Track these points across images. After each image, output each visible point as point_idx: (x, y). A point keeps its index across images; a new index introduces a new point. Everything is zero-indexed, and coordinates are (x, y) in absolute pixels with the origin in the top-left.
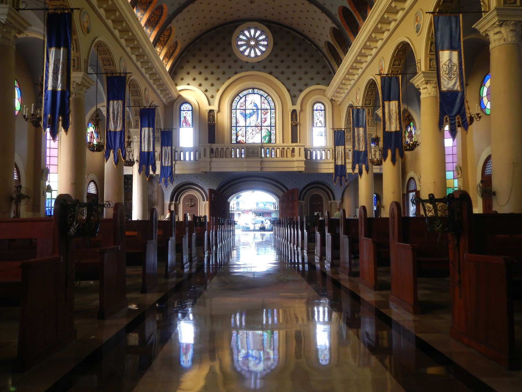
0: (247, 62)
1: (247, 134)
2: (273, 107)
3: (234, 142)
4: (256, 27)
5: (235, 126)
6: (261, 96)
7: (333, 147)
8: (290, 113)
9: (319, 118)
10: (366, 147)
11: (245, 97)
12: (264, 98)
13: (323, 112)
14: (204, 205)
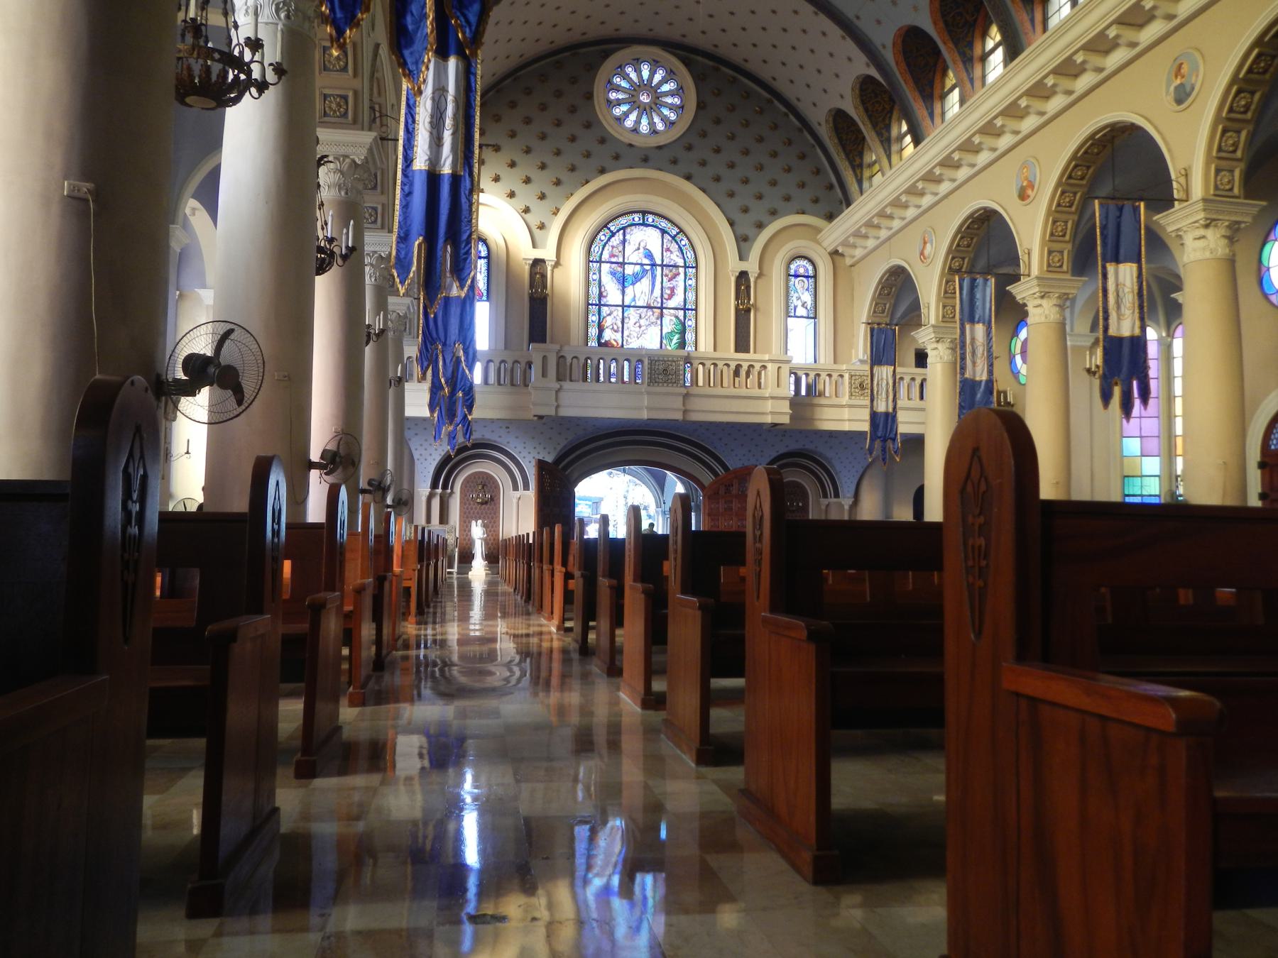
0: (631, 145)
1: (625, 325)
2: (691, 261)
3: (593, 344)
4: (654, 61)
5: (596, 305)
6: (663, 232)
7: (867, 367)
8: (733, 279)
9: (801, 295)
10: (990, 372)
11: (622, 231)
12: (670, 239)
13: (811, 280)
14: (515, 501)
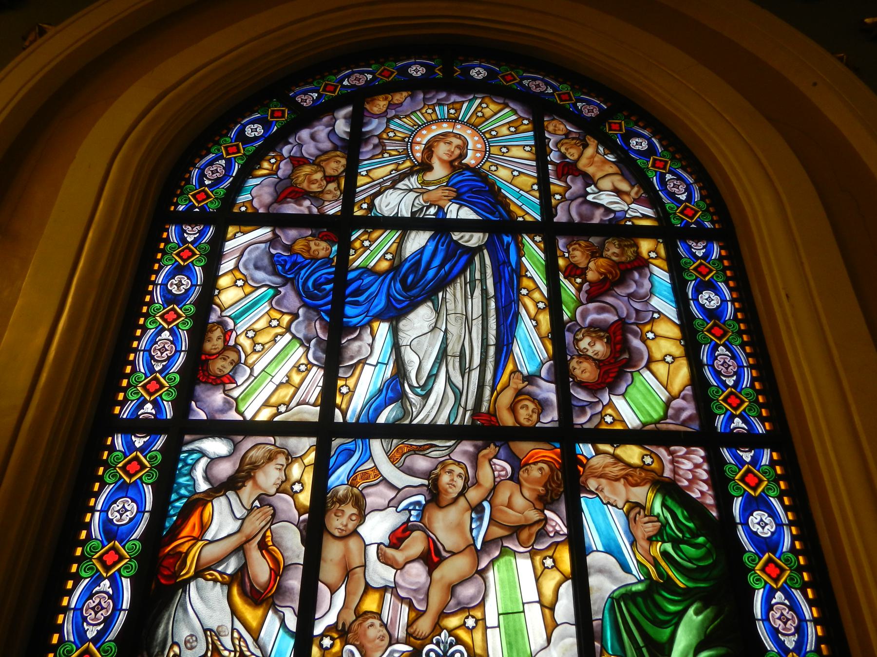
1: (332, 551)
5: (151, 427)
11: (349, 109)
